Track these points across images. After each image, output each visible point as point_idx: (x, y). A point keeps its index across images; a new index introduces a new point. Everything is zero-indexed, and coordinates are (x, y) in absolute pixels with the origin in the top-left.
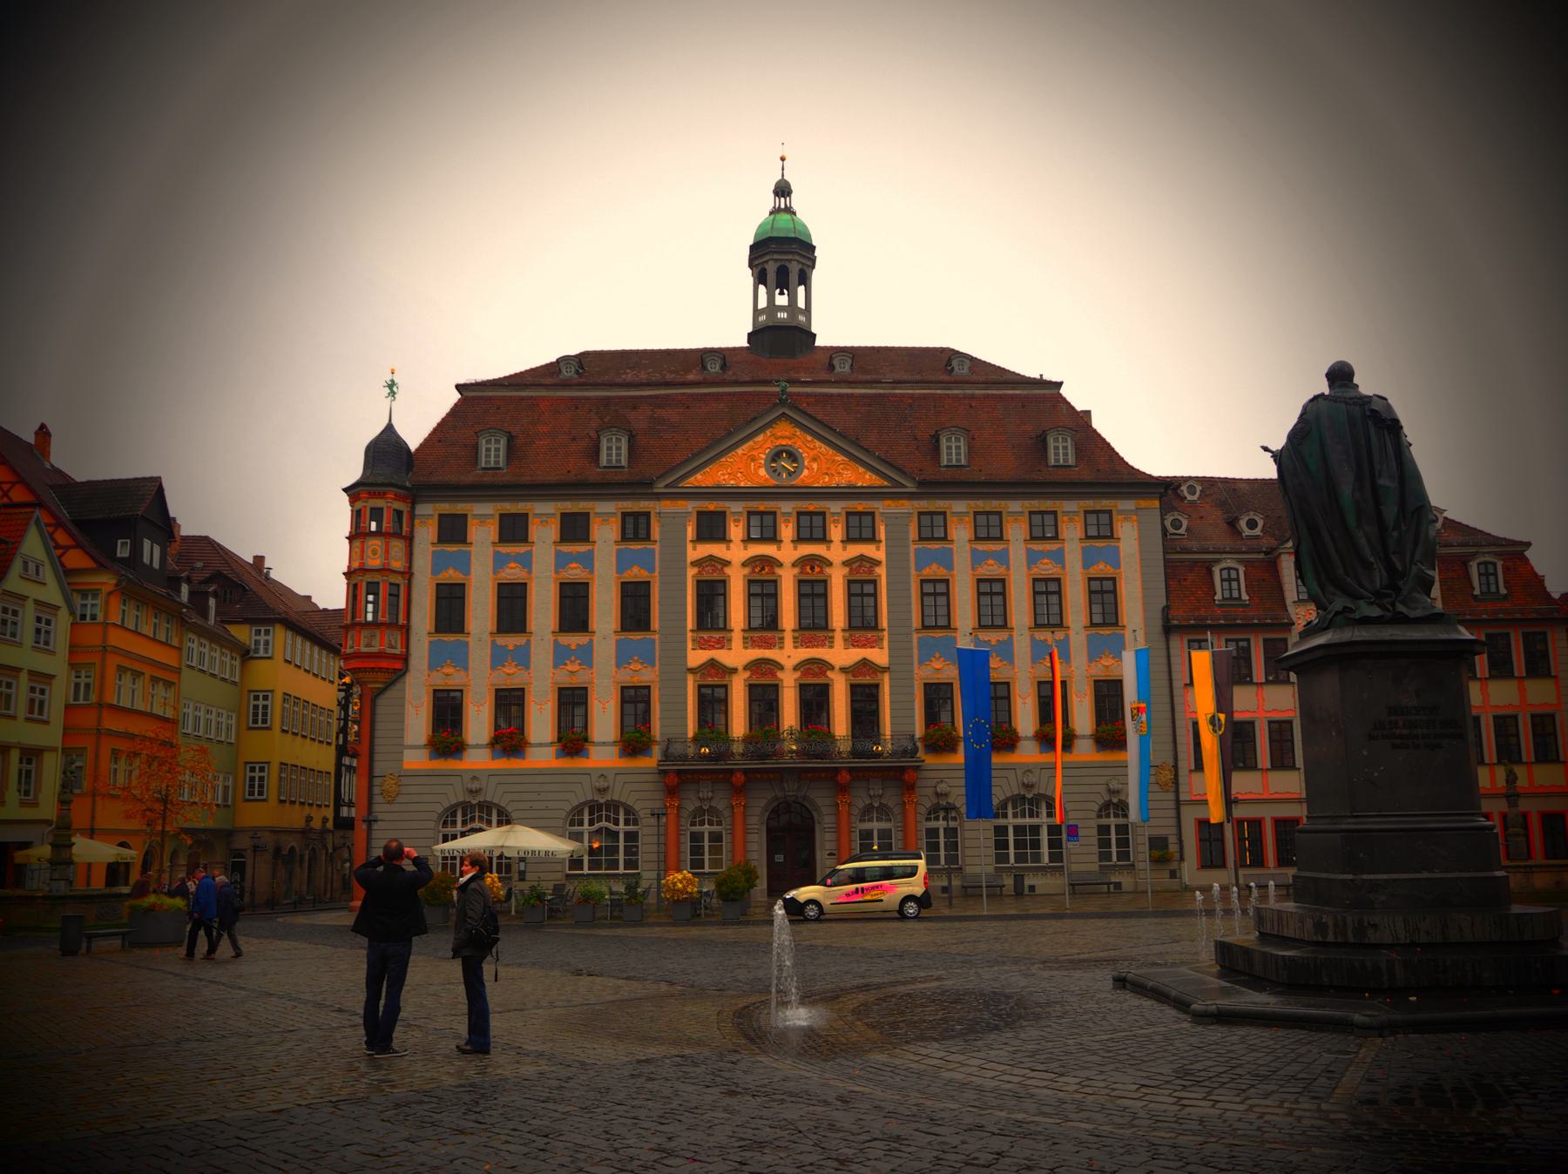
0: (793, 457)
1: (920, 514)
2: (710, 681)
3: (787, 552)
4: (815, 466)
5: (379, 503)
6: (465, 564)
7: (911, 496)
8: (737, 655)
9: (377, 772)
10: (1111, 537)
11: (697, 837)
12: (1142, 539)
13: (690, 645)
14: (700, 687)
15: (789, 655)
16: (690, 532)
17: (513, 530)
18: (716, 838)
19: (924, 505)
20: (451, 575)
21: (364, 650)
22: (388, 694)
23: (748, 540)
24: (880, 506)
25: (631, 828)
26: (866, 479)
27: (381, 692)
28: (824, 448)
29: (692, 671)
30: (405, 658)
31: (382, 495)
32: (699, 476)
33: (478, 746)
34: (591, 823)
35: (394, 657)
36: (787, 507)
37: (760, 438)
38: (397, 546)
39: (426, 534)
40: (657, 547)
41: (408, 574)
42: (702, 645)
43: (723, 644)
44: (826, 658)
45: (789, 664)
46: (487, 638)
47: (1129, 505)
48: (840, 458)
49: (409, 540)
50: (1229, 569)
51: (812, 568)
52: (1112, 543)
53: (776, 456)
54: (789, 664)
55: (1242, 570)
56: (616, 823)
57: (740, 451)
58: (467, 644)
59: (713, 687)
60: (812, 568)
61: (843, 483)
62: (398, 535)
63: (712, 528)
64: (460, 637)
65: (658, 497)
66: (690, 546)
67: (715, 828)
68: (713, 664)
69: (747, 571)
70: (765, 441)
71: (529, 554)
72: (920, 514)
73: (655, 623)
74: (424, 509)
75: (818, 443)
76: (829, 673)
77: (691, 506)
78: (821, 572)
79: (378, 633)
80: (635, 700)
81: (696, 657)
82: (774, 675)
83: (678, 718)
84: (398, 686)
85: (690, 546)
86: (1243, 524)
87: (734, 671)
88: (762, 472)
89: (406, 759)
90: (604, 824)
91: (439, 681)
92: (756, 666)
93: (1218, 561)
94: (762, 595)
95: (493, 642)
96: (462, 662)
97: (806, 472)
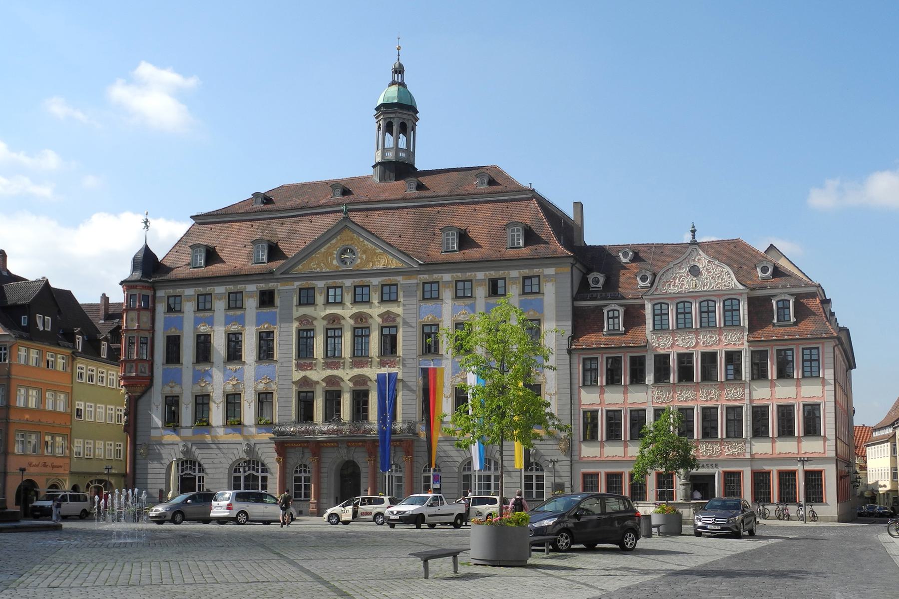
0: (352, 251)
1: (424, 283)
2: (304, 389)
3: (347, 312)
4: (364, 257)
5: (135, 292)
6: (180, 324)
7: (418, 272)
8: (317, 375)
9: (138, 442)
10: (539, 293)
11: (298, 480)
12: (557, 293)
13: (294, 369)
14: (299, 393)
15: (346, 374)
16: (295, 300)
17: (204, 305)
18: (307, 480)
19: (426, 277)
20: (173, 332)
21: (128, 375)
22: (144, 399)
23: (327, 303)
24: (400, 279)
25: (264, 474)
26: (394, 264)
27: (140, 397)
28: (370, 245)
29: (293, 383)
30: (151, 378)
31: (135, 287)
32: (300, 267)
33: (186, 427)
34: (245, 472)
35: (143, 378)
36: (348, 283)
37: (334, 241)
38: (146, 316)
39: (161, 308)
40: (278, 310)
41: (153, 330)
42: (299, 367)
43: (310, 366)
44: (367, 374)
45: (346, 378)
46: (191, 366)
47: (550, 271)
48: (379, 251)
49: (153, 311)
50: (613, 310)
51: (361, 320)
52: (539, 297)
53: (344, 252)
54: (346, 378)
55: (622, 310)
56: (257, 471)
57: (323, 250)
58: (181, 369)
59: (307, 392)
60: (361, 320)
61: (381, 267)
62: (146, 308)
63: (307, 297)
64: (178, 366)
65: (277, 280)
66: (295, 308)
67: (307, 475)
68: (305, 381)
69: (325, 322)
70: (336, 243)
71: (212, 317)
72: (424, 283)
73: (276, 357)
74: (161, 293)
75: (366, 242)
76: (369, 383)
77: (297, 284)
78: (366, 322)
79: (134, 365)
80: (264, 399)
81: (297, 375)
82: (339, 384)
83: (285, 411)
84: (148, 394)
85: (295, 308)
86: (600, 285)
87: (317, 383)
88: (335, 262)
89: (152, 435)
90: (251, 472)
91: (168, 390)
92: (330, 380)
93: (606, 306)
94: (334, 337)
95: (194, 369)
96: (179, 382)
97: (359, 261)
